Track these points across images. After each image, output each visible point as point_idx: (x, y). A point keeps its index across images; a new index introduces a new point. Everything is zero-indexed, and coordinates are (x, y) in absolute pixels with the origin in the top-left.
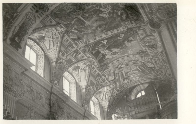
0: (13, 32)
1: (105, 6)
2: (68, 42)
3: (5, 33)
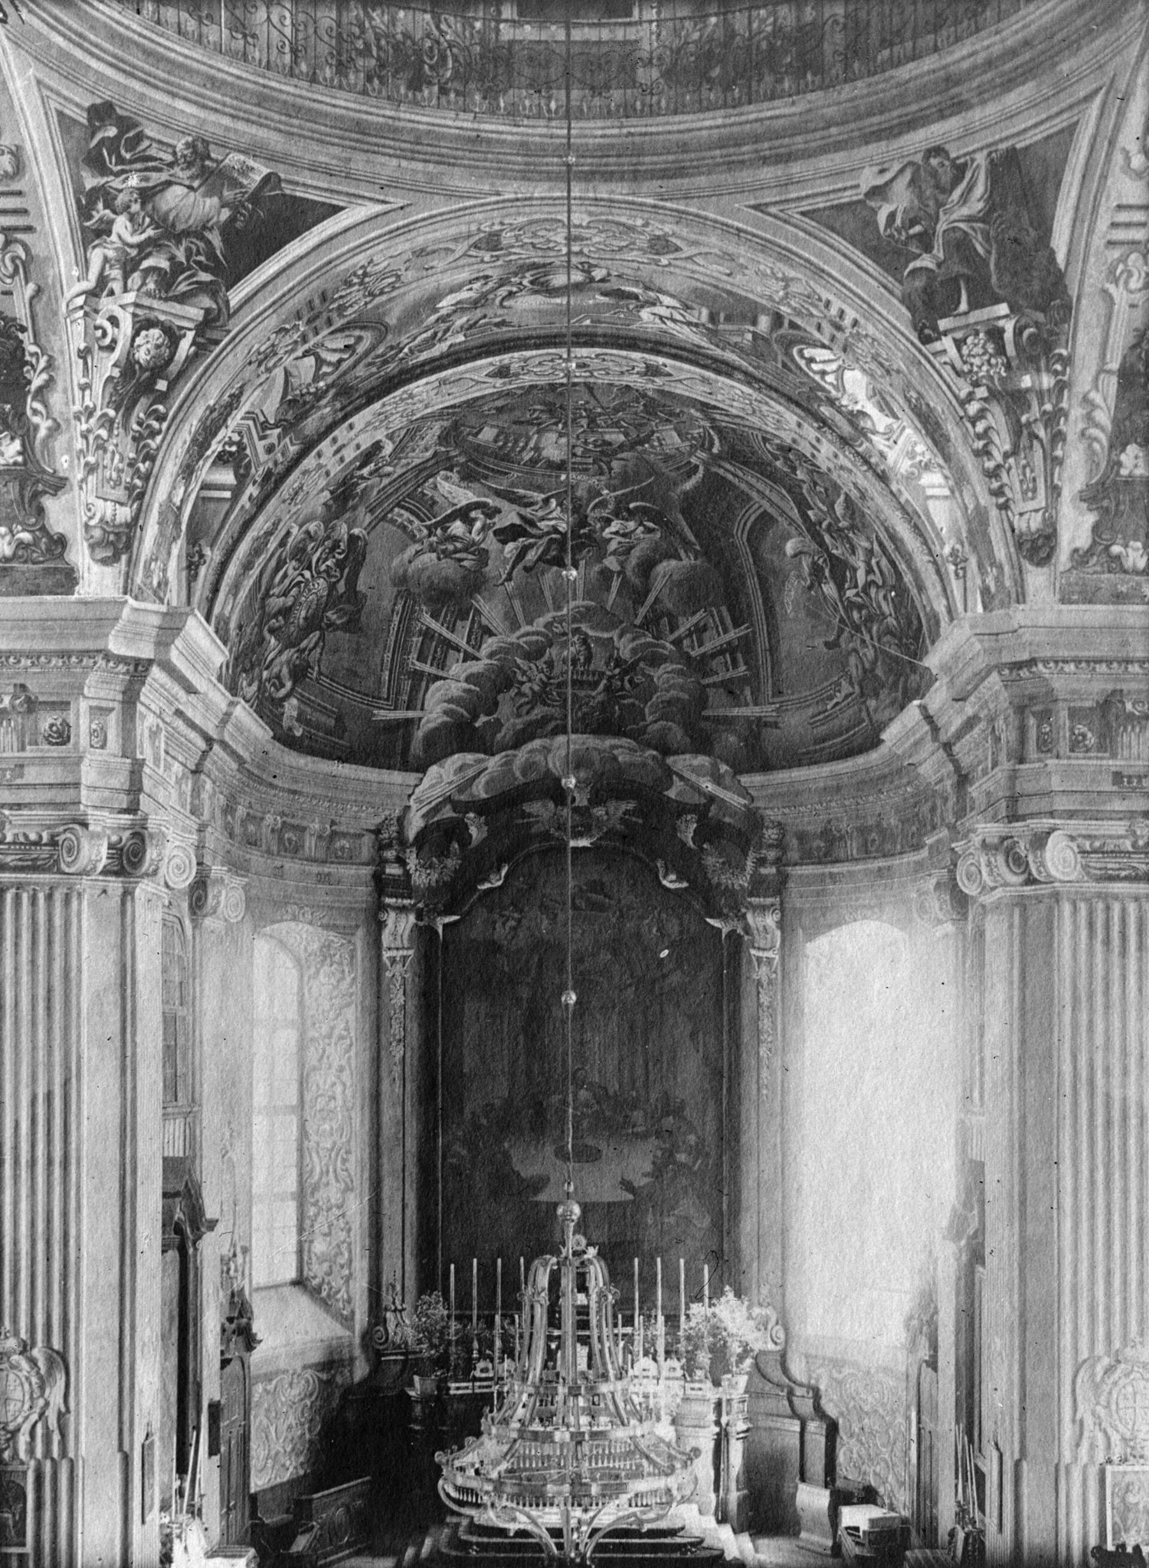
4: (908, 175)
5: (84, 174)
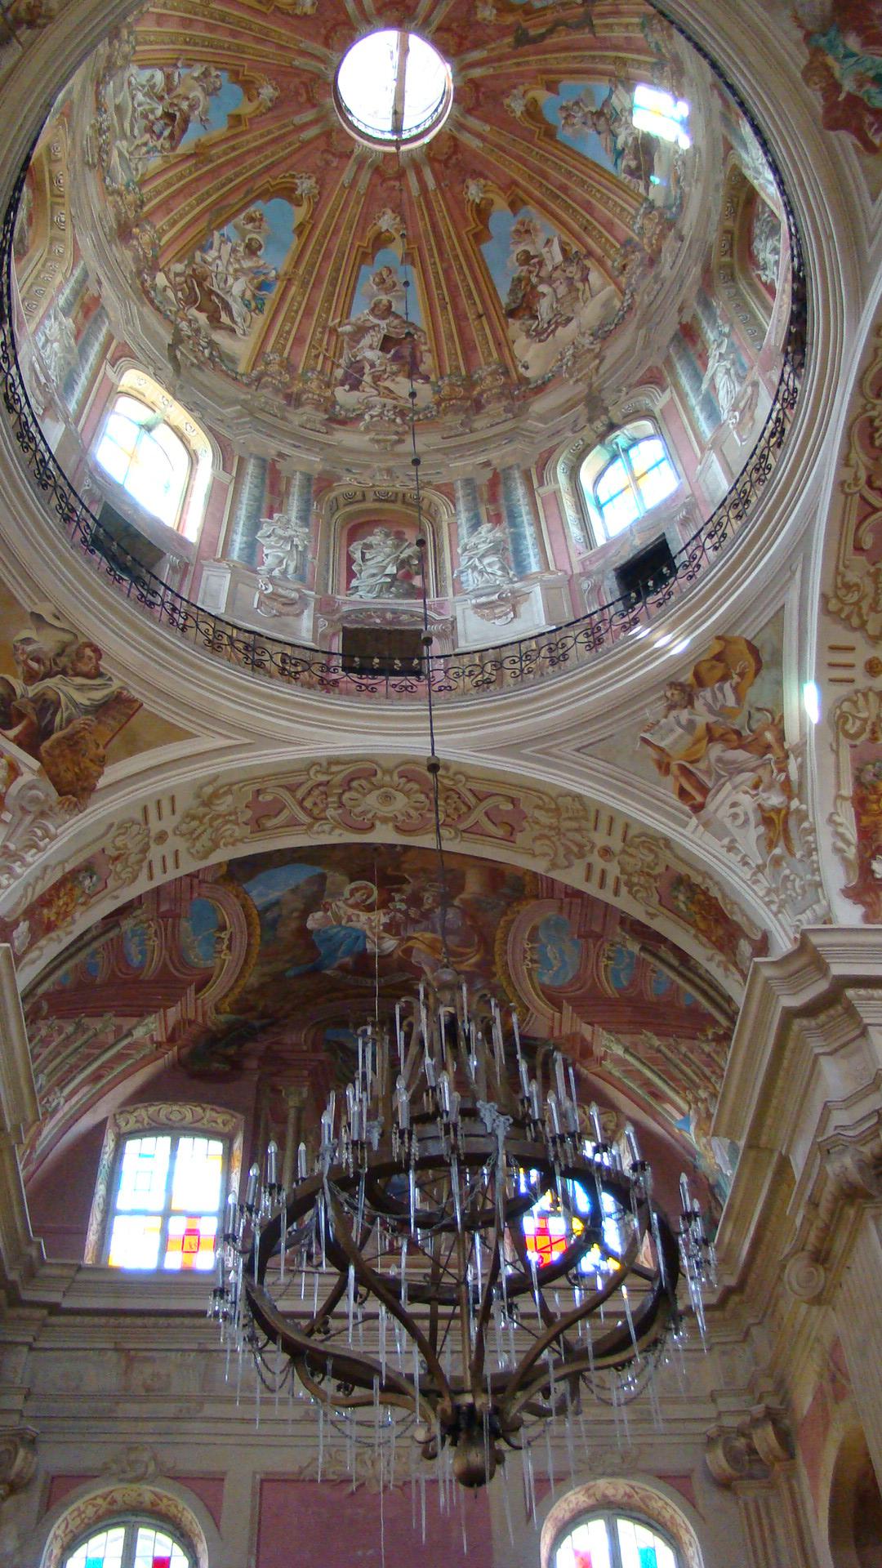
0: (837, 850)
3: (810, 885)
4: (67, 637)
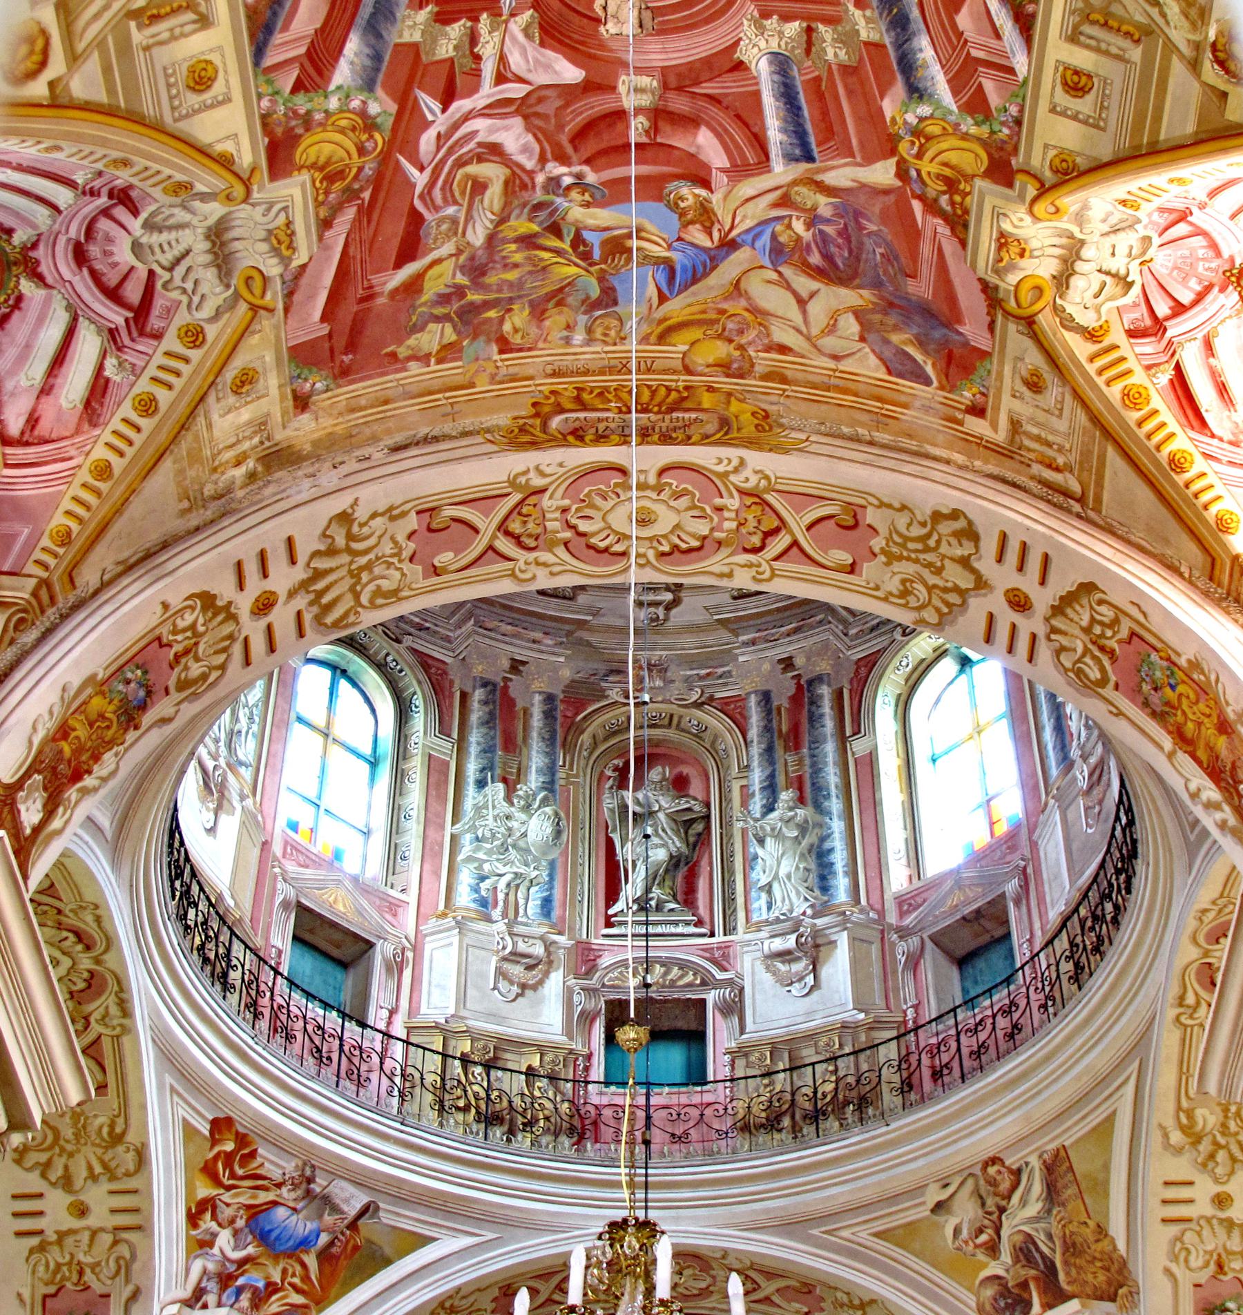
1: (467, 176)
2: (1082, 59)
5: (198, 1183)
